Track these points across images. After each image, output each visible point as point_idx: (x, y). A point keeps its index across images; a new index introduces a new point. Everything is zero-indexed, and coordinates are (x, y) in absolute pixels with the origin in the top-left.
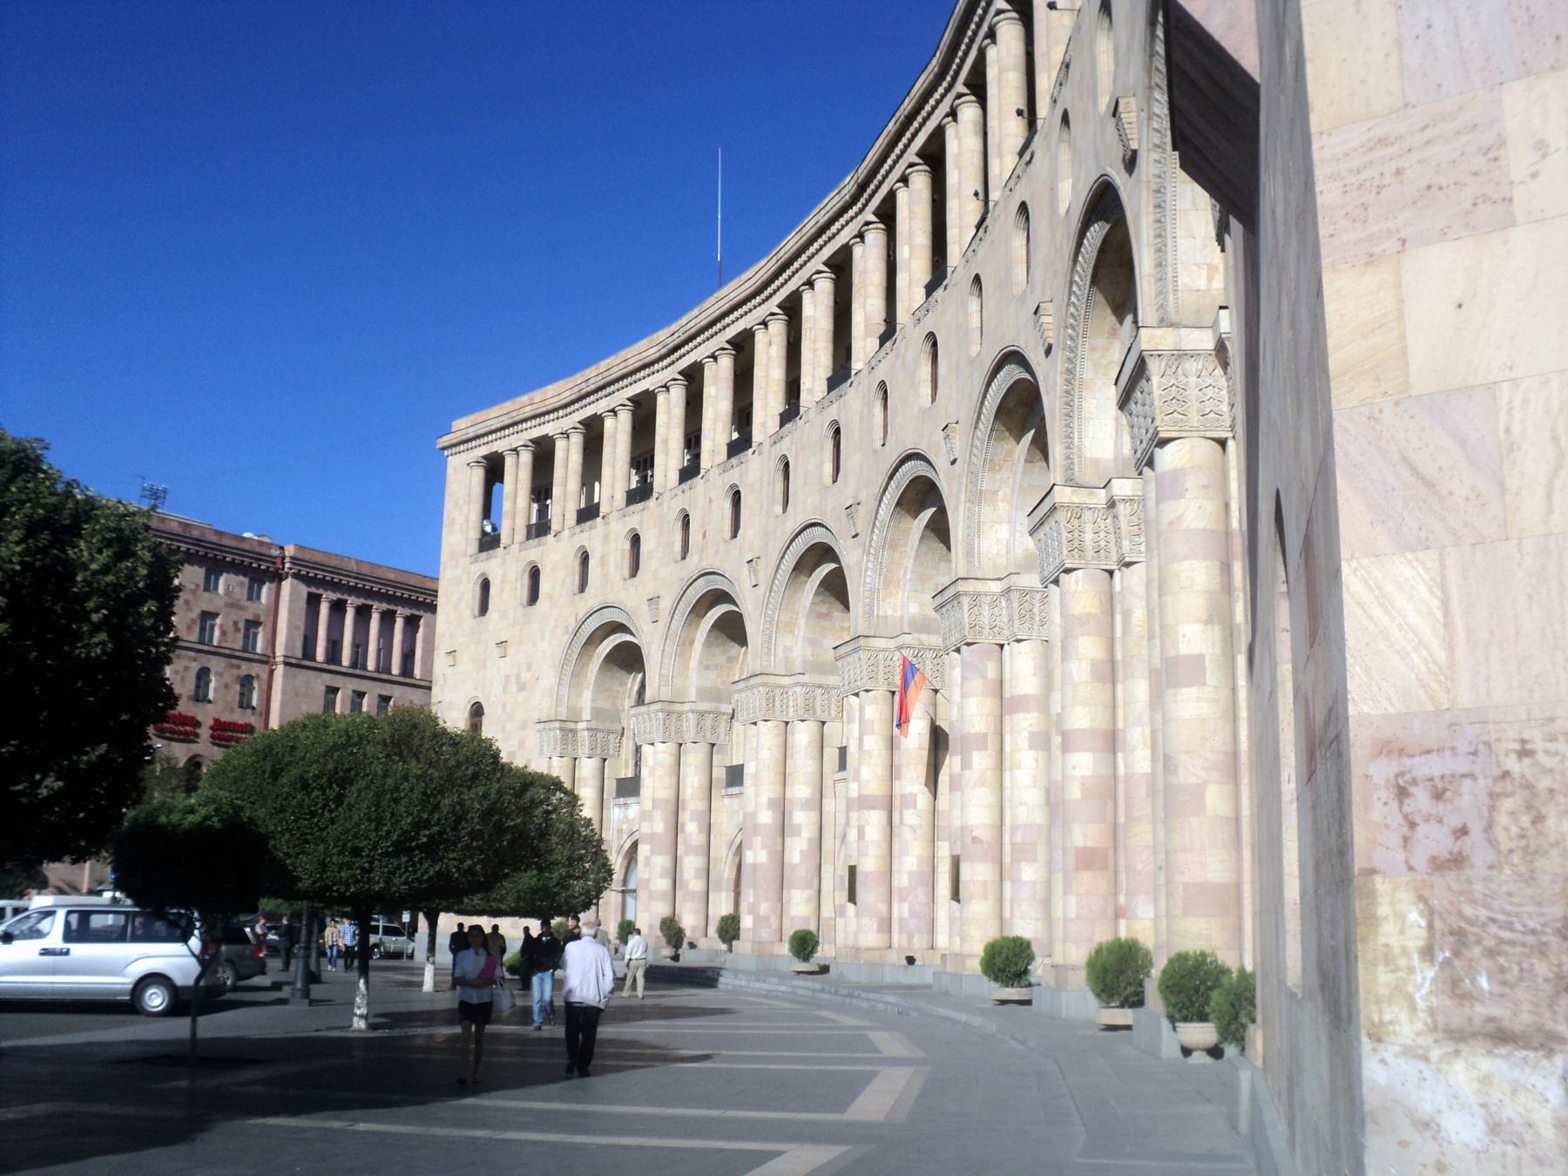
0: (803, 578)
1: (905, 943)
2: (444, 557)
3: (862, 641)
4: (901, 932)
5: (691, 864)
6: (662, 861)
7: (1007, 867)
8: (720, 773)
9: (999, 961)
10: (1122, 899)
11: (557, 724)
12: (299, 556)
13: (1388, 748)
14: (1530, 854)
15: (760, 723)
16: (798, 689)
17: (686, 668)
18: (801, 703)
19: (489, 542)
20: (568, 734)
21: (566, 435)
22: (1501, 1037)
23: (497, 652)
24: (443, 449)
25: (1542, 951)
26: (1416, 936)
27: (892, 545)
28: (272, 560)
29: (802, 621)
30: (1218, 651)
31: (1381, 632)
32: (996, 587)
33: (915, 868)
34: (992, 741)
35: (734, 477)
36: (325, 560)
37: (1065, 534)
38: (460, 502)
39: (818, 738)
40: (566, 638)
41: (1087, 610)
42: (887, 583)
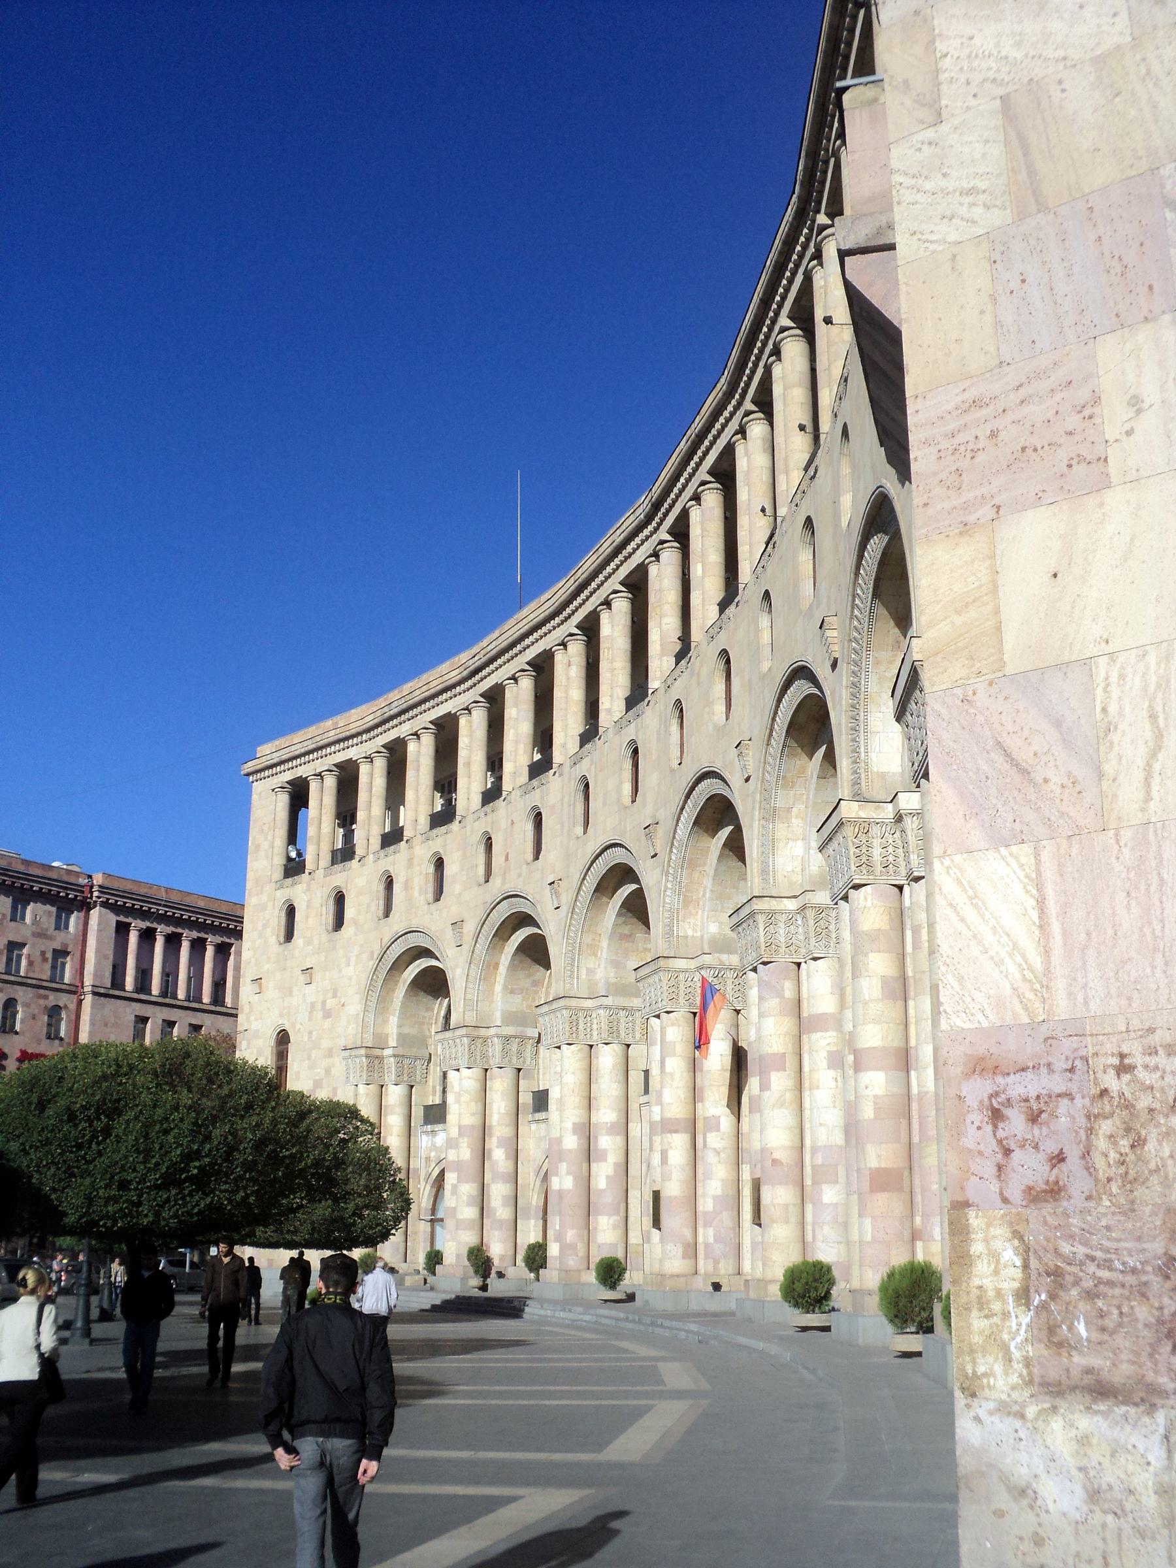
0: (605, 899)
1: (710, 1269)
2: (249, 885)
3: (662, 962)
4: (706, 1257)
5: (498, 1192)
6: (468, 1189)
7: (808, 1189)
8: (526, 1098)
9: (798, 1286)
10: (918, 1220)
11: (363, 1051)
12: (107, 884)
13: (982, 1066)
14: (1130, 1182)
15: (564, 1047)
16: (601, 1012)
17: (492, 992)
18: (604, 1027)
19: (294, 868)
20: (374, 1061)
21: (370, 759)
22: (1100, 1390)
23: (303, 978)
24: (248, 775)
25: (1142, 1292)
26: (1011, 1279)
27: (690, 864)
28: (79, 888)
29: (604, 943)
31: (975, 936)
32: (791, 905)
33: (719, 1192)
34: (791, 1062)
35: (535, 798)
36: (135, 889)
37: (852, 850)
38: (266, 828)
39: (622, 1060)
40: (372, 964)
41: (877, 926)
42: (686, 903)
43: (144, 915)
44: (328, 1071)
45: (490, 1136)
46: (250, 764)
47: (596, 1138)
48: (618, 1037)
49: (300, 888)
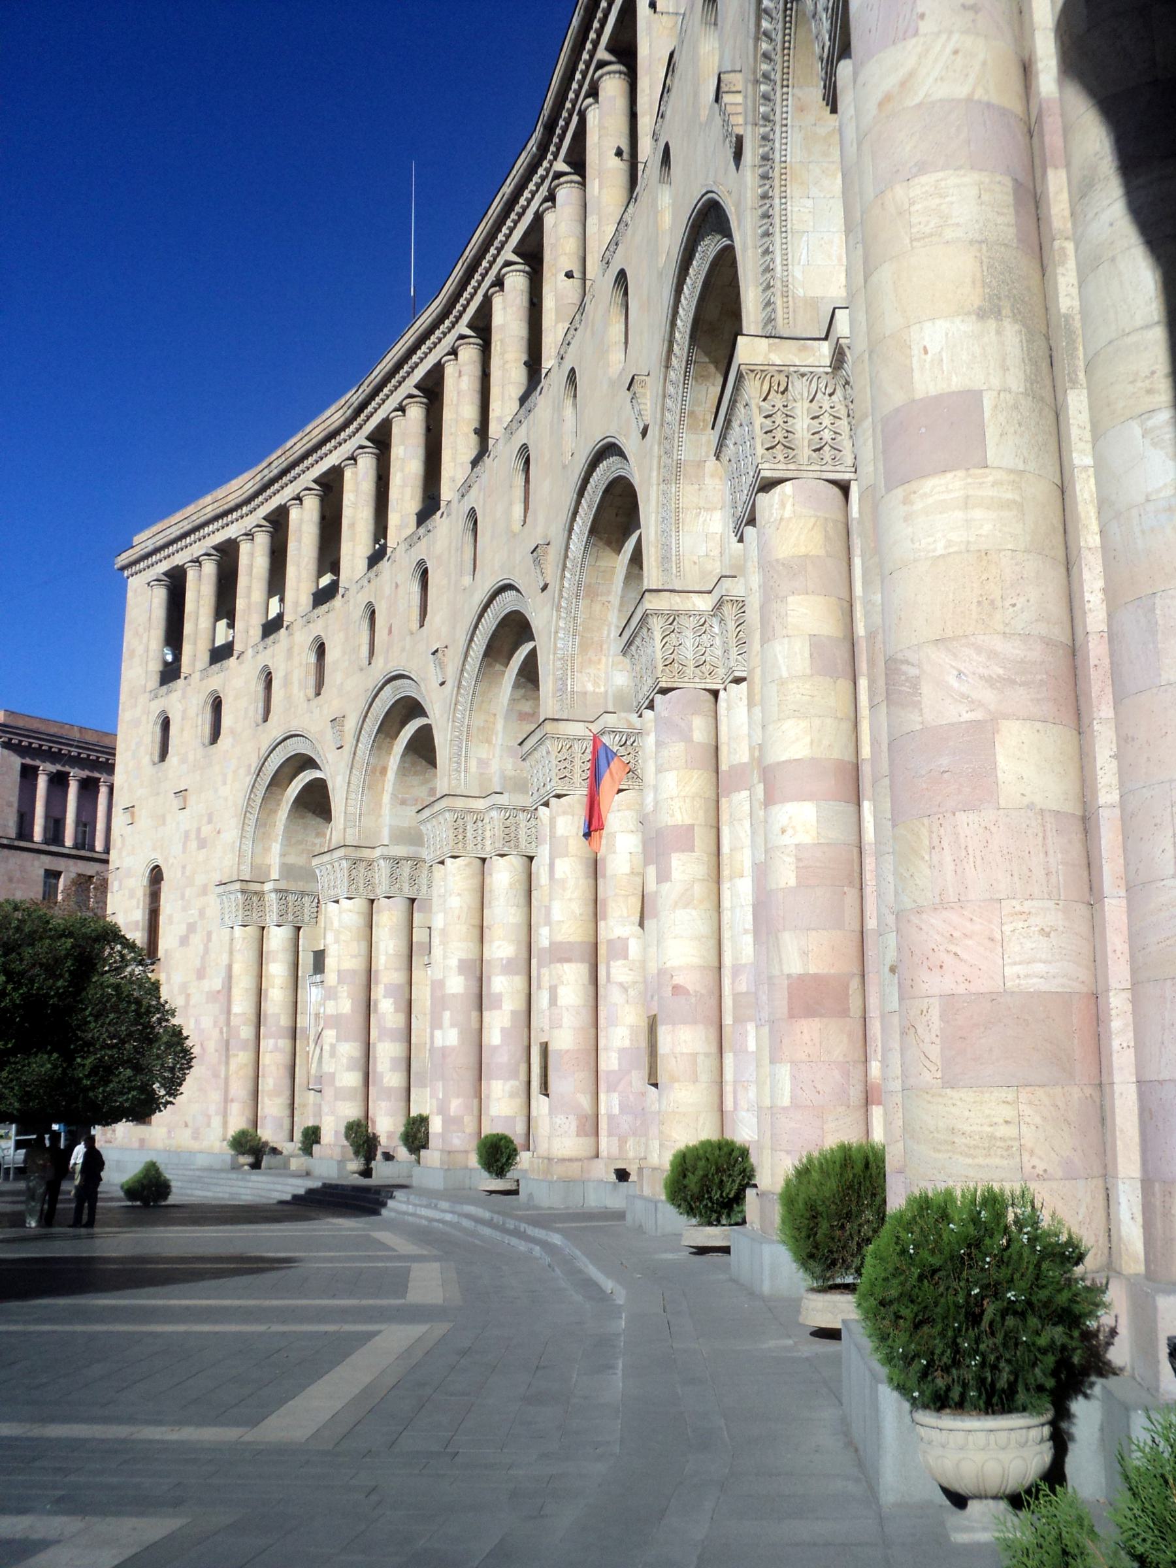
0: (498, 667)
1: (615, 1151)
2: (123, 697)
3: (549, 727)
4: (610, 1135)
5: (386, 1052)
6: (350, 1049)
7: (727, 1031)
9: (692, 1181)
10: (875, 1068)
11: (237, 886)
12: (10, 722)
15: (449, 861)
16: (494, 814)
17: (379, 804)
18: (499, 832)
19: (170, 673)
20: (252, 897)
21: (250, 535)
23: (176, 803)
24: (123, 568)
27: (587, 591)
29: (500, 725)
30: (1016, 381)
32: (703, 604)
33: (627, 1043)
34: (702, 838)
35: (420, 551)
36: (42, 728)
37: (758, 420)
38: (141, 630)
39: (524, 877)
40: (249, 780)
41: (803, 550)
42: (584, 647)
43: (54, 757)
44: (202, 913)
45: (377, 984)
46: (124, 556)
47: (489, 978)
48: (517, 846)
49: (175, 696)
